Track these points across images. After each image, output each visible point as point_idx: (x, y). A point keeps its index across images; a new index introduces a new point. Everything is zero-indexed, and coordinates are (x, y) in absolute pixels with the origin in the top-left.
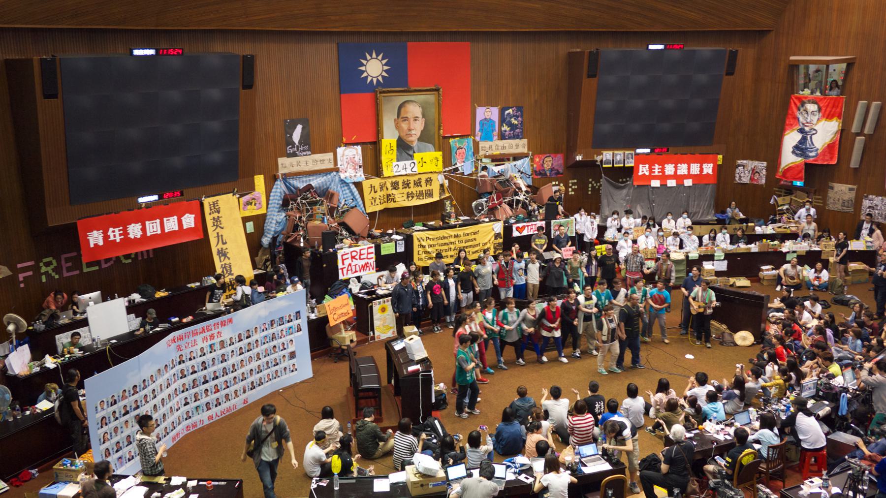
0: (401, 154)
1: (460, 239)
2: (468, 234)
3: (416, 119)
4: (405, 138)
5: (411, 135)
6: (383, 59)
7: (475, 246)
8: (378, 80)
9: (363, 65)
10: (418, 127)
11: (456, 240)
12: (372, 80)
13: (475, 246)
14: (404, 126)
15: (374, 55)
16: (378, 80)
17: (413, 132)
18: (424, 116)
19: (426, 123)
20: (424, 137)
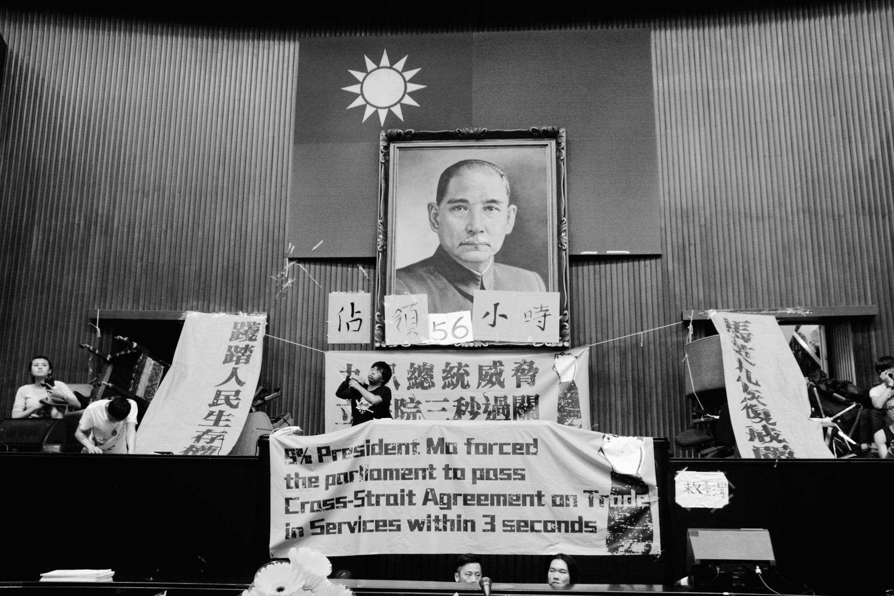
0: (443, 292)
1: (457, 461)
2: (488, 449)
3: (490, 205)
4: (457, 251)
5: (476, 247)
6: (407, 68)
7: (521, 500)
8: (391, 115)
9: (355, 81)
10: (497, 227)
11: (439, 460)
12: (375, 115)
13: (521, 500)
14: (456, 221)
15: (385, 61)
16: (391, 115)
17: (481, 238)
18: (513, 199)
19: (518, 217)
20: (517, 251)
